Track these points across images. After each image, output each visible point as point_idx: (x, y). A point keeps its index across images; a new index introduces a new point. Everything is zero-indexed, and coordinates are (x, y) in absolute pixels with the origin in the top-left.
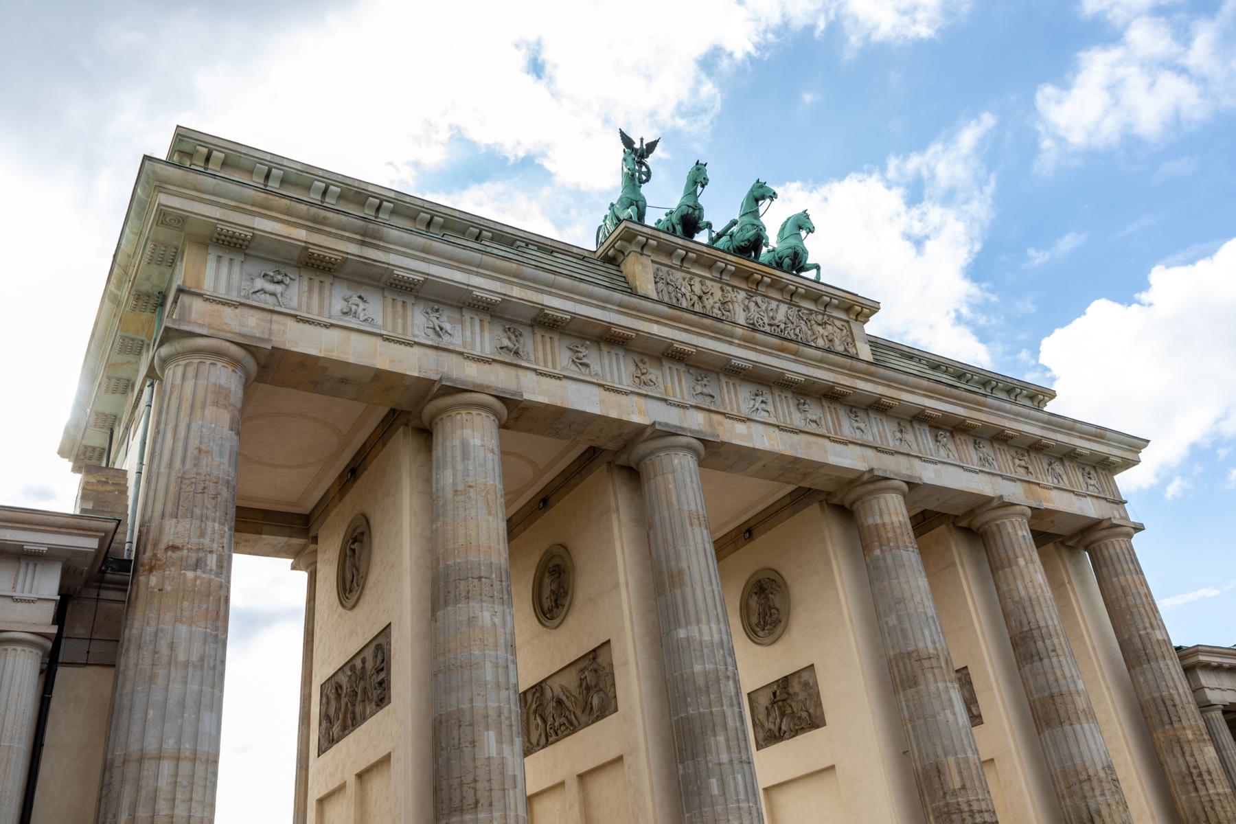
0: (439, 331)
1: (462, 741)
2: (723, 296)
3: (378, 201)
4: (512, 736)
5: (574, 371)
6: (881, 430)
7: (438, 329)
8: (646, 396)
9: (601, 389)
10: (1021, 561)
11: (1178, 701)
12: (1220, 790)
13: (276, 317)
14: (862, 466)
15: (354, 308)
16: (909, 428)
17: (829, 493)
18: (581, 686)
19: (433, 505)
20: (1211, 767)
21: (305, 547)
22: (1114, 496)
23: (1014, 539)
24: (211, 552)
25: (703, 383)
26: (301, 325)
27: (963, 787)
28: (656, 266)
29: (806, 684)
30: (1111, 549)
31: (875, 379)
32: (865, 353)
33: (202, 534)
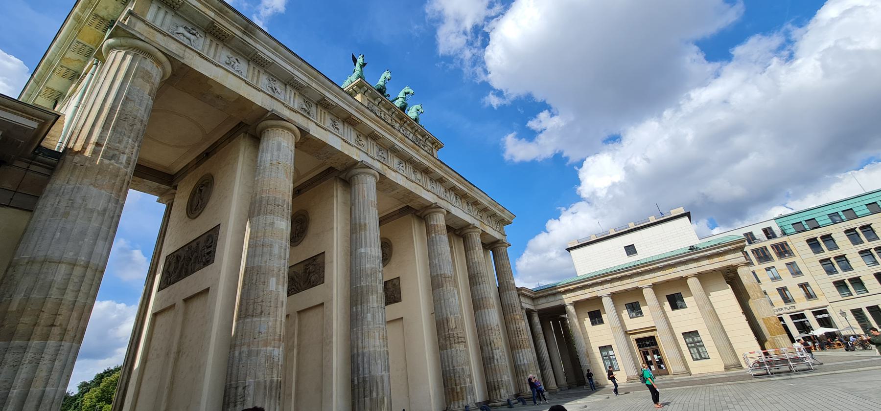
0: (274, 90)
1: (258, 281)
4: (284, 282)
5: (332, 129)
6: (439, 189)
8: (360, 149)
10: (477, 249)
11: (516, 306)
12: (525, 337)
13: (187, 50)
14: (433, 202)
15: (233, 63)
16: (448, 192)
17: (417, 210)
18: (305, 272)
19: (255, 168)
20: (524, 329)
21: (168, 190)
23: (475, 240)
24: (123, 153)
26: (202, 59)
27: (456, 327)
29: (395, 285)
30: (500, 250)
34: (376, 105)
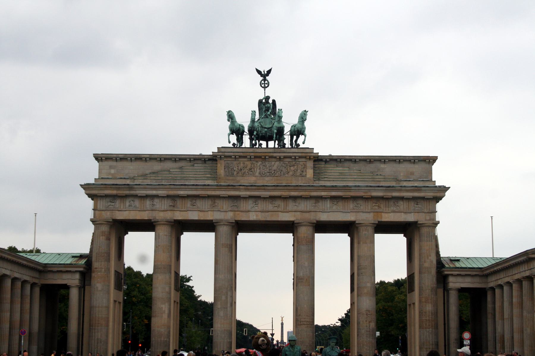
2: (251, 166)
3: (145, 159)
6: (303, 205)
7: (152, 205)
9: (199, 211)
10: (361, 243)
13: (114, 211)
14: (292, 219)
22: (429, 210)
24: (103, 268)
25: (234, 202)
27: (300, 315)
28: (225, 162)
31: (299, 190)
32: (310, 173)
33: (101, 265)
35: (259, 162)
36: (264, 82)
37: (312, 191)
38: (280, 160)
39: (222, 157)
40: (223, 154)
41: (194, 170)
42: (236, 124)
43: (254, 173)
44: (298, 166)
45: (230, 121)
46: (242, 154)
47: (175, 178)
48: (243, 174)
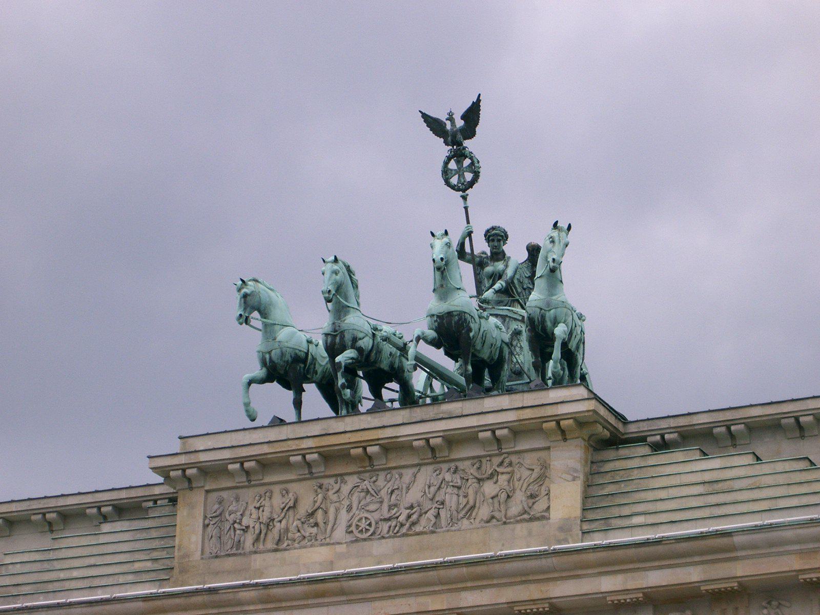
2: (315, 502)
28: (214, 496)
31: (495, 582)
34: (242, 487)
35: (346, 478)
36: (459, 162)
37: (556, 575)
38: (434, 457)
39: (189, 472)
40: (192, 459)
41: (95, 550)
42: (282, 335)
43: (326, 530)
44: (517, 476)
45: (247, 321)
46: (266, 449)
47: (14, 591)
48: (279, 541)
